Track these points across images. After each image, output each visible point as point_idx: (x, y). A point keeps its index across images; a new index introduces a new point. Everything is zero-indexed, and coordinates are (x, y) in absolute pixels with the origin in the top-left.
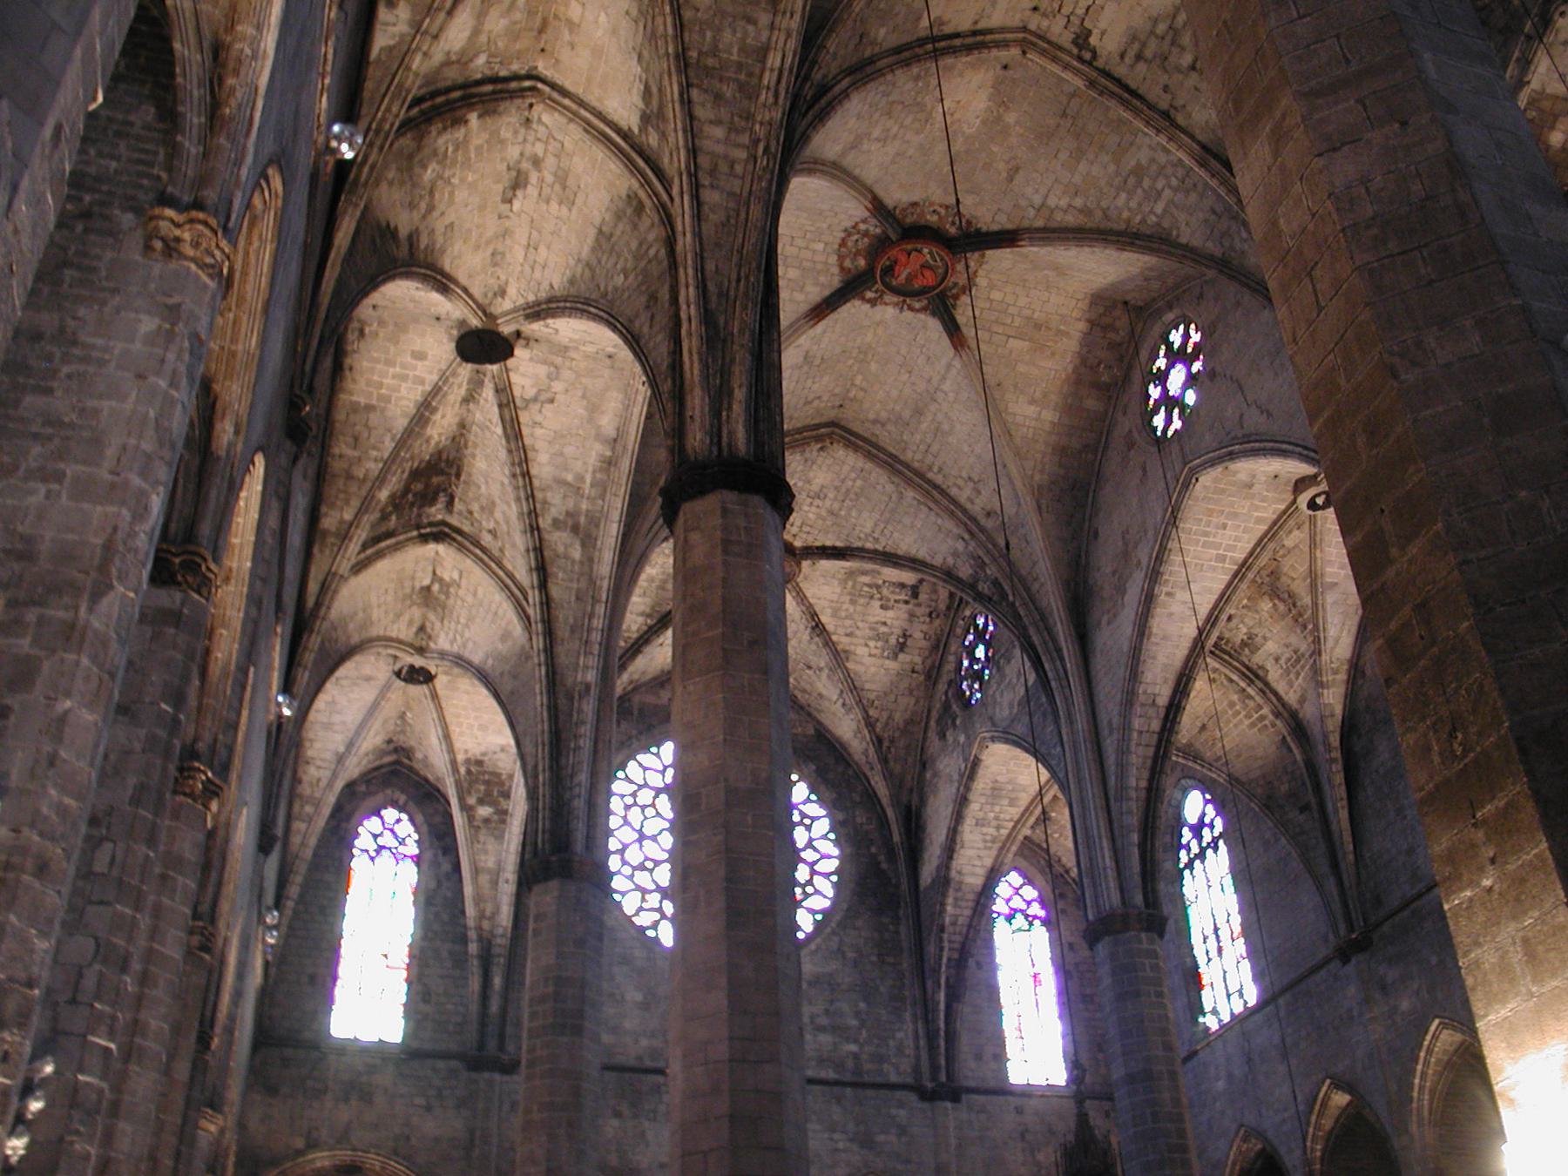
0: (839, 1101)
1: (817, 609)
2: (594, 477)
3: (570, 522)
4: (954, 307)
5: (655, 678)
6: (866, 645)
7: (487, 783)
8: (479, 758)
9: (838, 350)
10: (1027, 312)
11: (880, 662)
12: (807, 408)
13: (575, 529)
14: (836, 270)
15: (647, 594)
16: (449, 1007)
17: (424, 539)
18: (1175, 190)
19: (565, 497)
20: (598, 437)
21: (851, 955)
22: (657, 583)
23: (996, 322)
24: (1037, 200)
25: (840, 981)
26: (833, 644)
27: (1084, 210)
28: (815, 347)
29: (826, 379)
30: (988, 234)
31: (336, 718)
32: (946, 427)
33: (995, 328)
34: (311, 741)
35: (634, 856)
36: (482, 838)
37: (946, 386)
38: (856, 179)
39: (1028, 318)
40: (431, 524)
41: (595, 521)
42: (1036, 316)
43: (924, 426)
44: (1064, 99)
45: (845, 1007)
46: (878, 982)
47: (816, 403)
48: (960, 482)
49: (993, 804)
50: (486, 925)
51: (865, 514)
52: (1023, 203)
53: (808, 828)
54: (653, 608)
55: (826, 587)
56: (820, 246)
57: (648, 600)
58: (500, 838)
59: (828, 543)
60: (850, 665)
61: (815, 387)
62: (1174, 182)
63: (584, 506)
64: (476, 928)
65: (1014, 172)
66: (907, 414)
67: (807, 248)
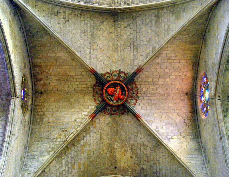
4: (96, 80)
9: (126, 50)
10: (74, 83)
12: (128, 23)
14: (137, 83)
18: (63, 171)
24: (92, 134)
28: (135, 53)
32: (83, 35)
33: (81, 77)
37: (88, 50)
44: (99, 170)
47: (126, 25)
52: (94, 130)
61: (128, 34)
62: (64, 173)
65: (100, 140)
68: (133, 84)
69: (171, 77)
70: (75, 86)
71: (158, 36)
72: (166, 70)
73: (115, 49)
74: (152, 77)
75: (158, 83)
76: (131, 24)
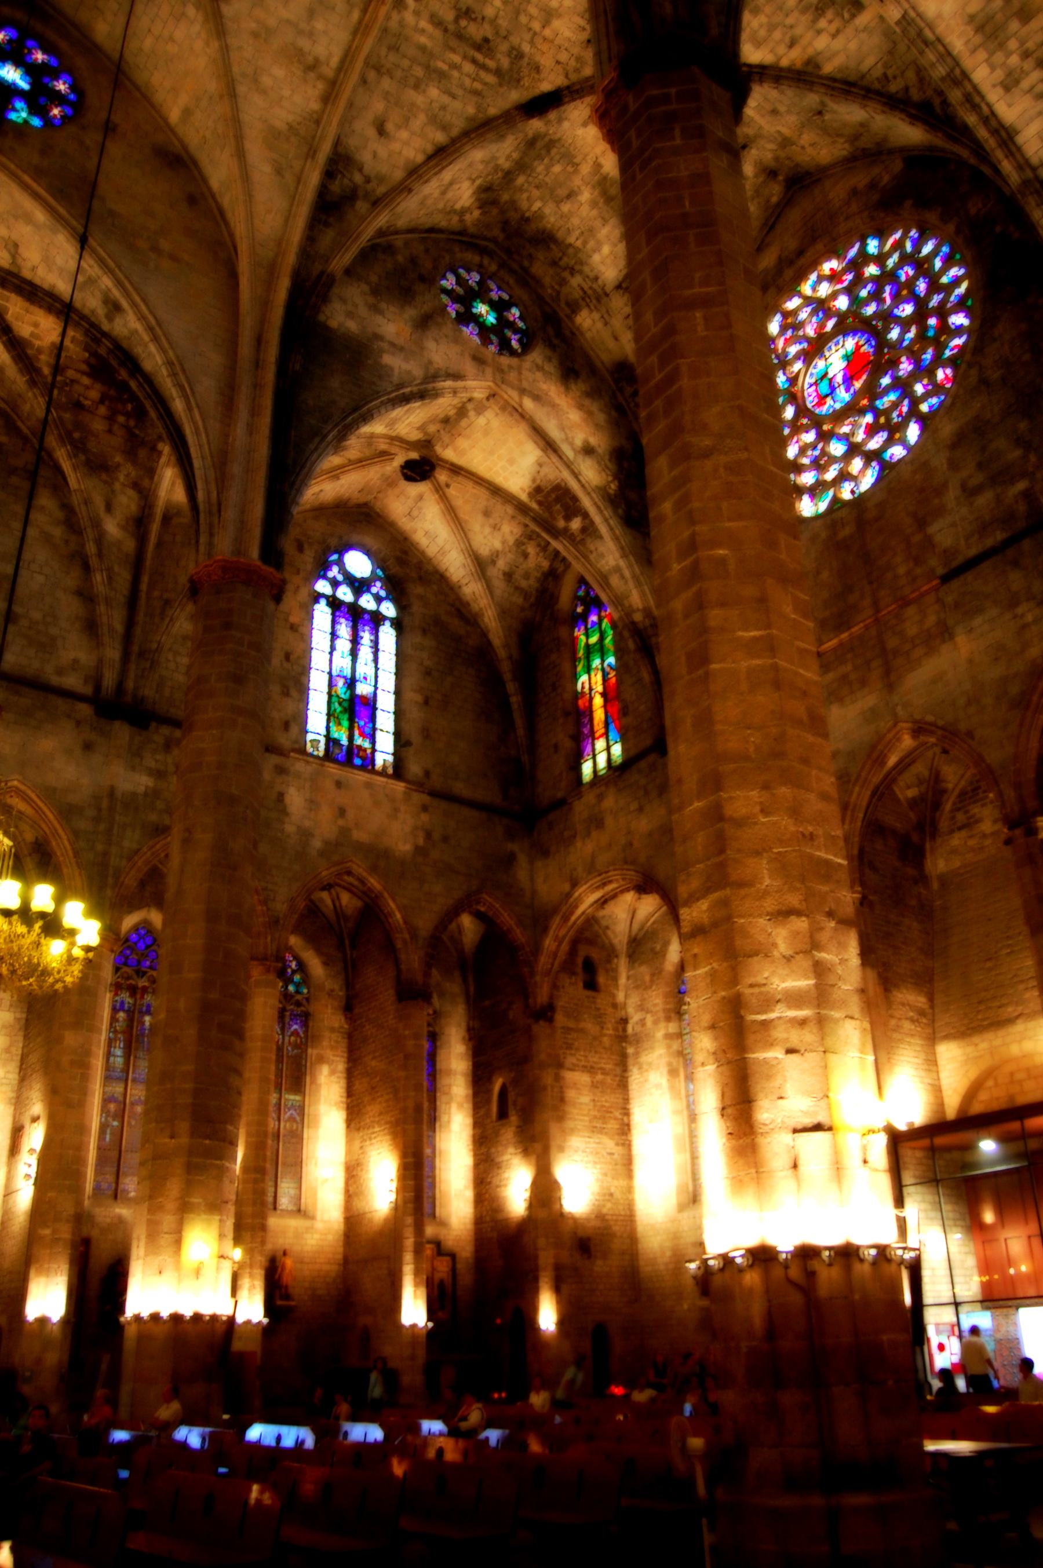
0: (1015, 564)
6: (819, 32)
8: (534, 486)
11: (849, 31)
26: (789, 70)
36: (592, 548)
45: (1001, 443)
49: (1001, 46)
57: (614, 221)
58: (601, 537)
60: (828, 69)
71: (255, 35)
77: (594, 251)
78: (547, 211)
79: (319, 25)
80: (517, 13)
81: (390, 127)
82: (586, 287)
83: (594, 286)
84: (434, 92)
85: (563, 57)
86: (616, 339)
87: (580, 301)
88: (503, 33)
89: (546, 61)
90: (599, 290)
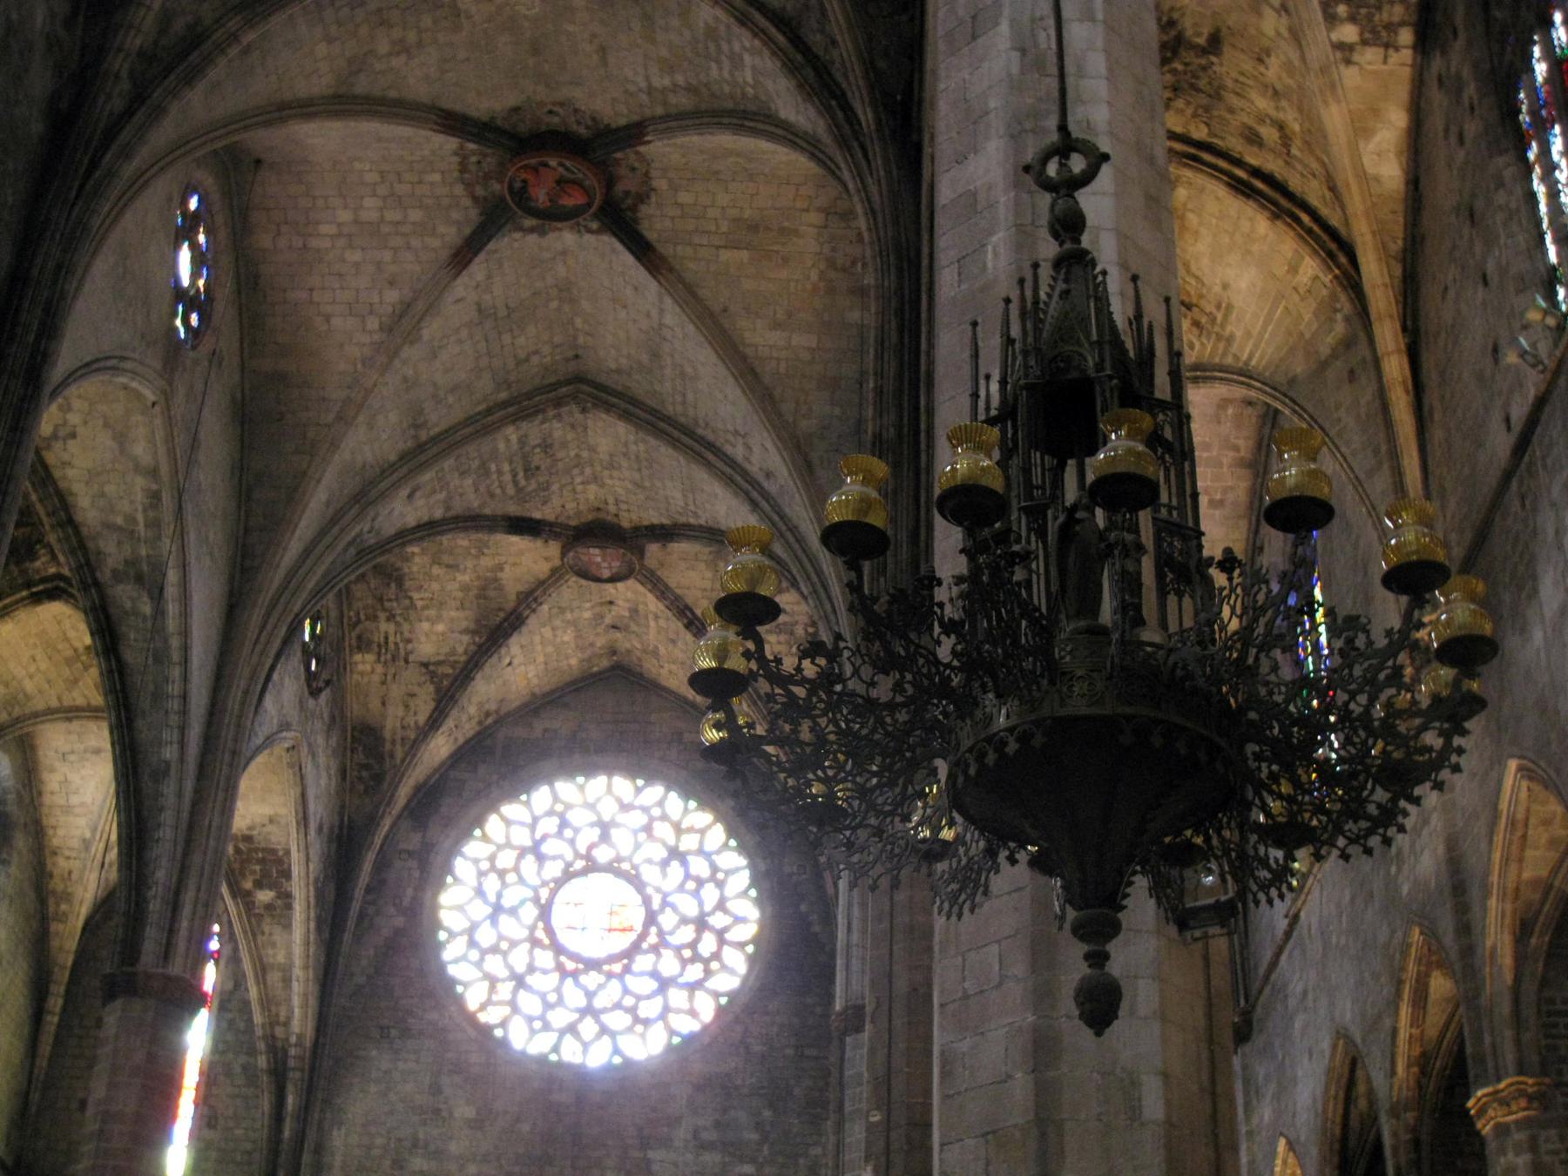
1: (689, 601)
2: (146, 518)
3: (132, 572)
4: (636, 221)
5: (525, 705)
7: (262, 861)
8: (247, 832)
10: (733, 212)
13: (139, 579)
14: (467, 202)
15: (467, 605)
16: (239, 1132)
17: (37, 599)
19: (119, 543)
20: (138, 469)
21: (757, 1048)
22: (475, 592)
23: (696, 230)
25: (739, 1082)
27: (691, 89)
28: (487, 297)
29: (531, 330)
30: (618, 129)
31: (74, 800)
32: (689, 370)
33: (696, 240)
34: (54, 828)
35: (486, 936)
36: (266, 929)
38: (400, 103)
39: (736, 220)
40: (44, 580)
41: (159, 569)
42: (747, 214)
43: (668, 371)
45: (742, 1116)
46: (792, 1082)
47: (535, 360)
48: (731, 438)
50: (279, 1032)
51: (669, 484)
52: (632, 88)
53: (720, 885)
54: (477, 621)
55: (692, 574)
56: (437, 177)
58: (288, 926)
59: (656, 521)
61: (521, 341)
63: (143, 552)
64: (265, 1037)
65: (602, 50)
66: (645, 358)
67: (420, 182)
68: (485, 199)
69: (332, 230)
70: (723, 199)
71: (405, 379)
72: (356, 256)
73: (566, 291)
74: (407, 229)
75: (380, 203)
76: (511, 364)
77: (428, 619)
78: (417, 559)
79: (451, 399)
80: (576, 466)
81: (418, 494)
82: (391, 639)
83: (401, 645)
84: (469, 481)
85: (570, 506)
86: (384, 704)
87: (375, 645)
88: (553, 471)
89: (556, 501)
90: (402, 652)
